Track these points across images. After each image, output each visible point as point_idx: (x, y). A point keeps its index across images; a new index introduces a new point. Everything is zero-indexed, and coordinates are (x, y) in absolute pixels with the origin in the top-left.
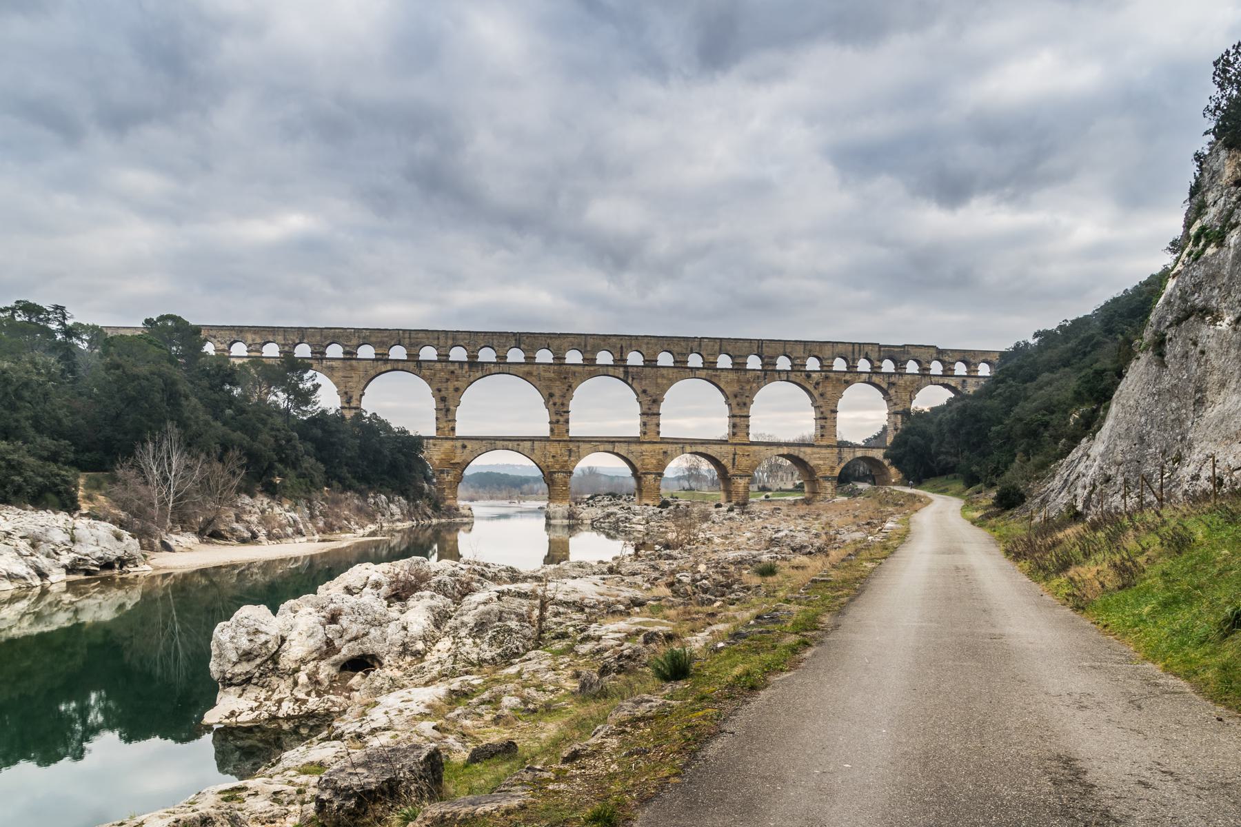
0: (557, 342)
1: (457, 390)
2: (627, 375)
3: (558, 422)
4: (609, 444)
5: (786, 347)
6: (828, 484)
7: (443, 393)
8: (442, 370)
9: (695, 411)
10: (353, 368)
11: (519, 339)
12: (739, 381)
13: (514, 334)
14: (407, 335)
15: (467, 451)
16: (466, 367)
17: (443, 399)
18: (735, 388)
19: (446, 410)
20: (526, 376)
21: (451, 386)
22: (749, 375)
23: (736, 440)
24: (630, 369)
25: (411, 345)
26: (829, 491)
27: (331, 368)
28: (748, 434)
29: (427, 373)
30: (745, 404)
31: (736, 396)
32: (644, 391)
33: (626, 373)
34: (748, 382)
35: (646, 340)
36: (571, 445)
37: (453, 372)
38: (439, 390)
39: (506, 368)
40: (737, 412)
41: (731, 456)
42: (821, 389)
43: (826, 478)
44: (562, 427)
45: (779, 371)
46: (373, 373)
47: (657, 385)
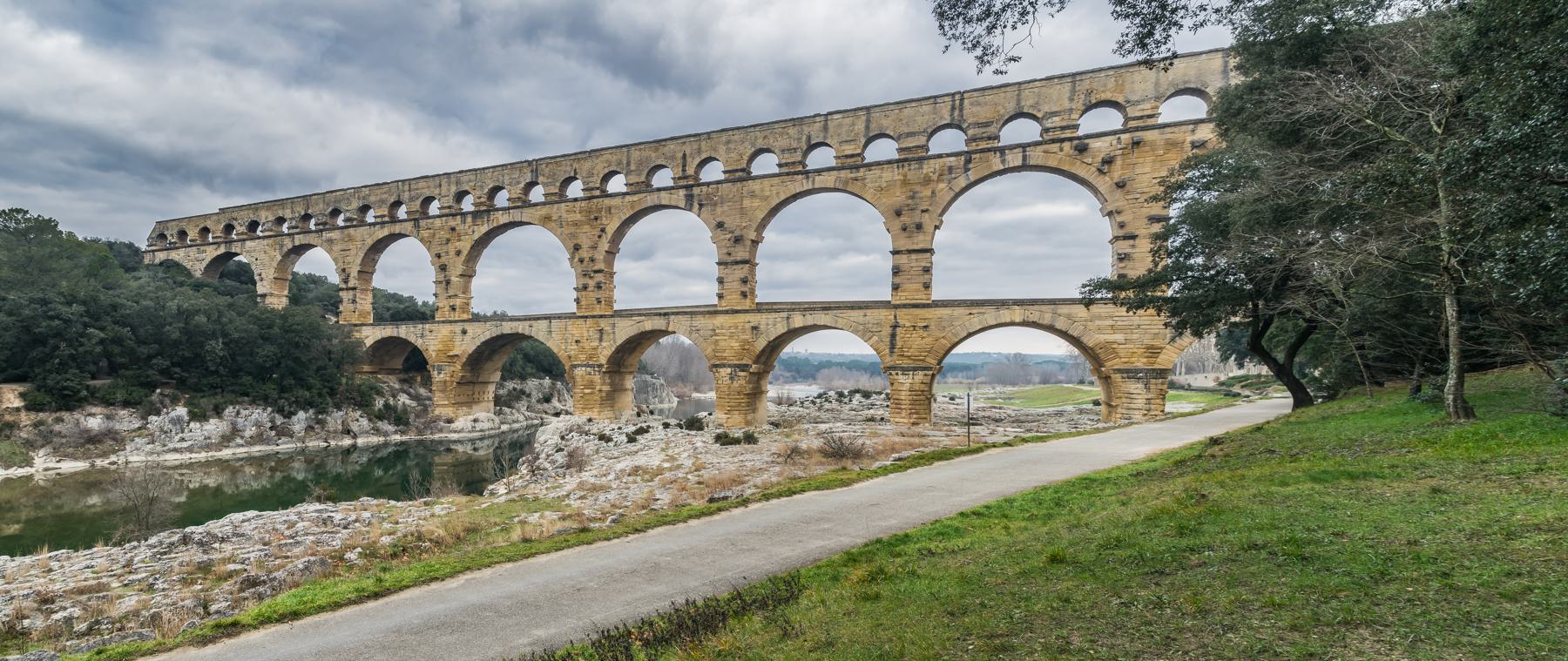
0: (587, 165)
3: (585, 288)
6: (1136, 387)
7: (443, 260)
8: (442, 228)
10: (351, 239)
12: (905, 182)
15: (467, 338)
16: (469, 219)
17: (443, 268)
18: (899, 197)
20: (546, 221)
21: (452, 248)
22: (929, 168)
23: (902, 298)
25: (412, 199)
26: (1140, 402)
27: (330, 241)
28: (927, 286)
29: (425, 234)
30: (919, 227)
31: (898, 214)
32: (720, 225)
33: (689, 198)
34: (927, 181)
35: (724, 137)
36: (603, 323)
37: (453, 229)
38: (439, 256)
39: (516, 216)
40: (905, 244)
42: (1117, 172)
43: (1131, 374)
44: (592, 295)
46: (370, 242)
47: (743, 212)
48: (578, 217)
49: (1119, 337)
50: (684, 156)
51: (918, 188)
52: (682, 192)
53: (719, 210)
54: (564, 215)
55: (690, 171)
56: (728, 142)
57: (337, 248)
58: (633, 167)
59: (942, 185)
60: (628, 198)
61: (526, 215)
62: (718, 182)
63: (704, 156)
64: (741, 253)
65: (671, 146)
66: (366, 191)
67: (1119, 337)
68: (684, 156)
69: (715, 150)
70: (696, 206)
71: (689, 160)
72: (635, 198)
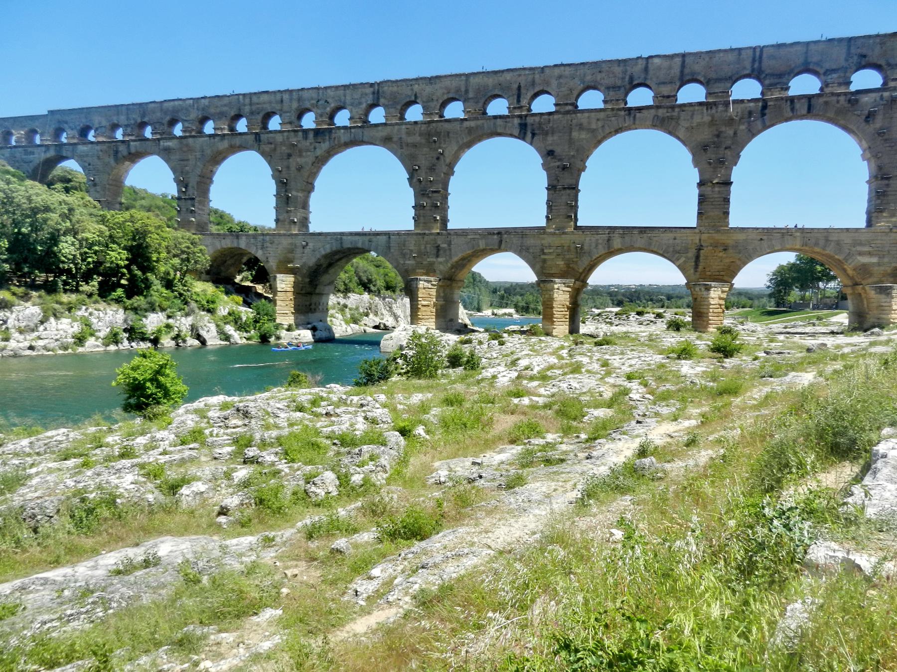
1: (300, 169)
2: (526, 128)
4: (498, 240)
5: (806, 57)
8: (282, 143)
9: (640, 180)
11: (377, 94)
12: (712, 123)
13: (372, 85)
14: (247, 101)
16: (311, 135)
18: (705, 135)
19: (292, 194)
20: (386, 142)
24: (530, 120)
29: (267, 148)
34: (731, 121)
35: (557, 71)
41: (692, 254)
45: (792, 100)
47: (571, 141)
48: (417, 139)
49: (874, 260)
50: (519, 88)
51: (723, 129)
52: (517, 121)
53: (550, 139)
54: (404, 136)
55: (524, 102)
56: (560, 77)
57: (175, 157)
58: (471, 95)
59: (743, 127)
60: (466, 124)
61: (368, 133)
62: (550, 114)
63: (537, 89)
64: (567, 180)
65: (508, 76)
66: (206, 102)
67: (874, 260)
68: (519, 88)
69: (548, 83)
70: (529, 135)
71: (523, 91)
72: (472, 124)
